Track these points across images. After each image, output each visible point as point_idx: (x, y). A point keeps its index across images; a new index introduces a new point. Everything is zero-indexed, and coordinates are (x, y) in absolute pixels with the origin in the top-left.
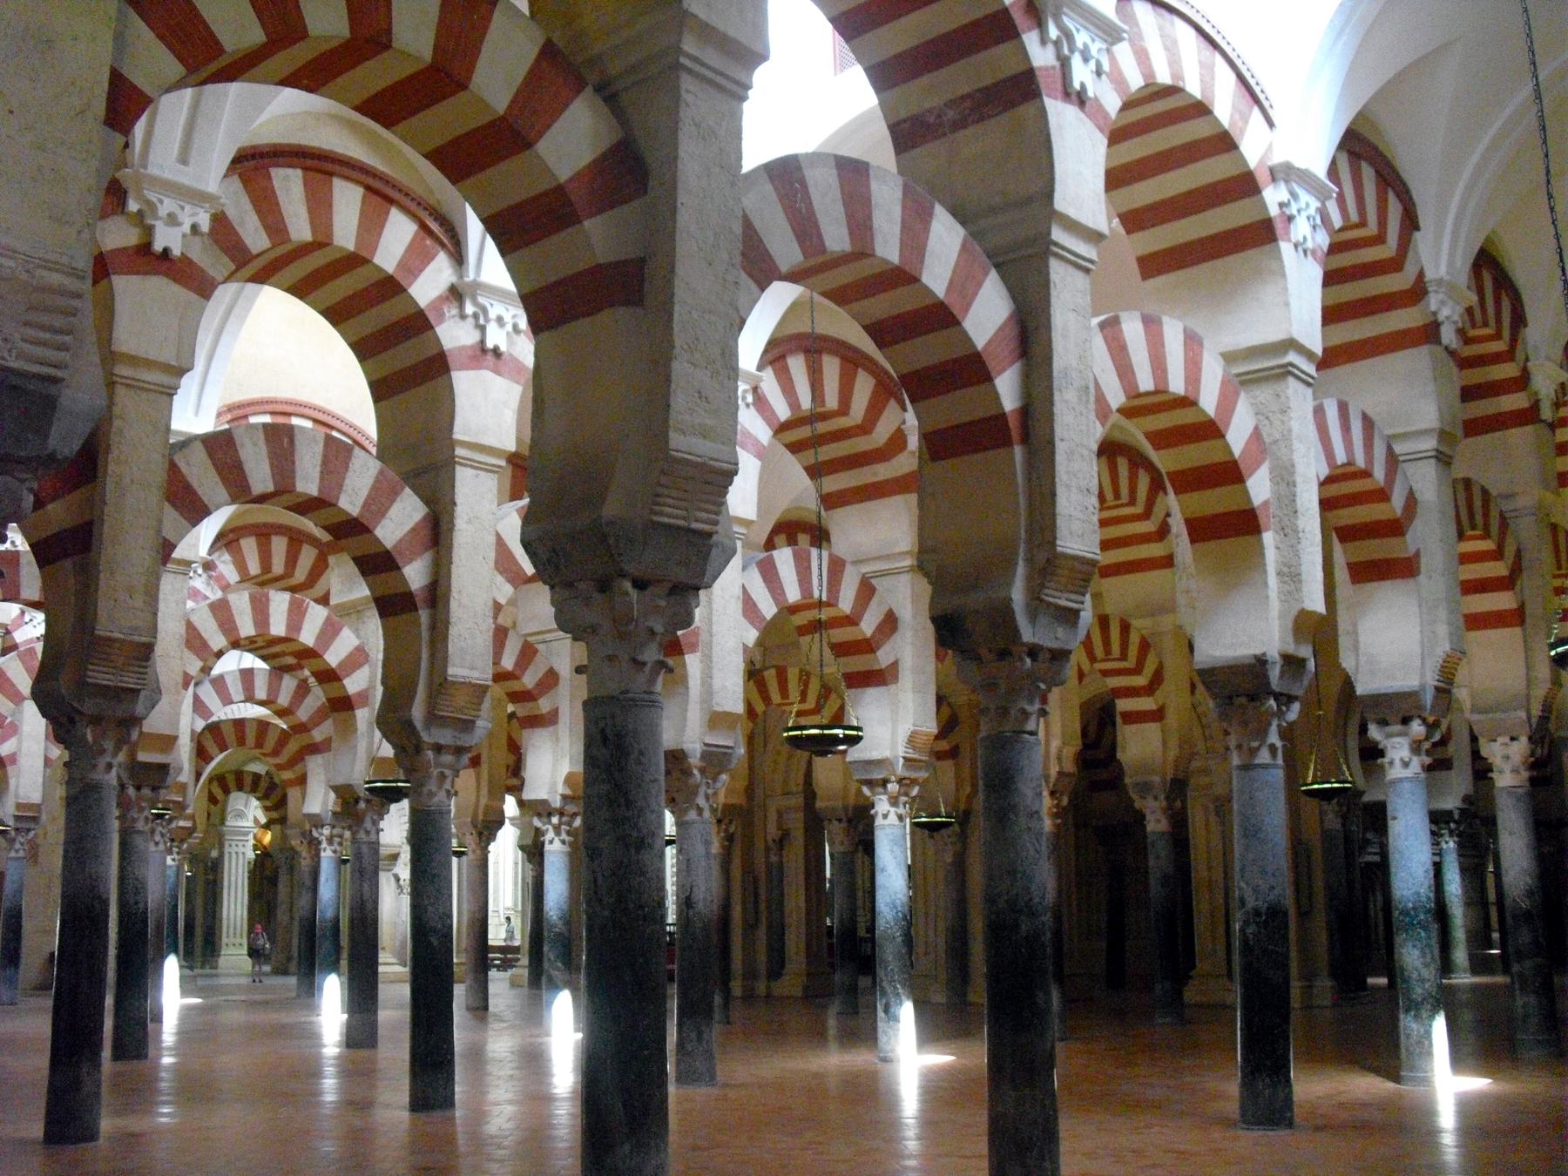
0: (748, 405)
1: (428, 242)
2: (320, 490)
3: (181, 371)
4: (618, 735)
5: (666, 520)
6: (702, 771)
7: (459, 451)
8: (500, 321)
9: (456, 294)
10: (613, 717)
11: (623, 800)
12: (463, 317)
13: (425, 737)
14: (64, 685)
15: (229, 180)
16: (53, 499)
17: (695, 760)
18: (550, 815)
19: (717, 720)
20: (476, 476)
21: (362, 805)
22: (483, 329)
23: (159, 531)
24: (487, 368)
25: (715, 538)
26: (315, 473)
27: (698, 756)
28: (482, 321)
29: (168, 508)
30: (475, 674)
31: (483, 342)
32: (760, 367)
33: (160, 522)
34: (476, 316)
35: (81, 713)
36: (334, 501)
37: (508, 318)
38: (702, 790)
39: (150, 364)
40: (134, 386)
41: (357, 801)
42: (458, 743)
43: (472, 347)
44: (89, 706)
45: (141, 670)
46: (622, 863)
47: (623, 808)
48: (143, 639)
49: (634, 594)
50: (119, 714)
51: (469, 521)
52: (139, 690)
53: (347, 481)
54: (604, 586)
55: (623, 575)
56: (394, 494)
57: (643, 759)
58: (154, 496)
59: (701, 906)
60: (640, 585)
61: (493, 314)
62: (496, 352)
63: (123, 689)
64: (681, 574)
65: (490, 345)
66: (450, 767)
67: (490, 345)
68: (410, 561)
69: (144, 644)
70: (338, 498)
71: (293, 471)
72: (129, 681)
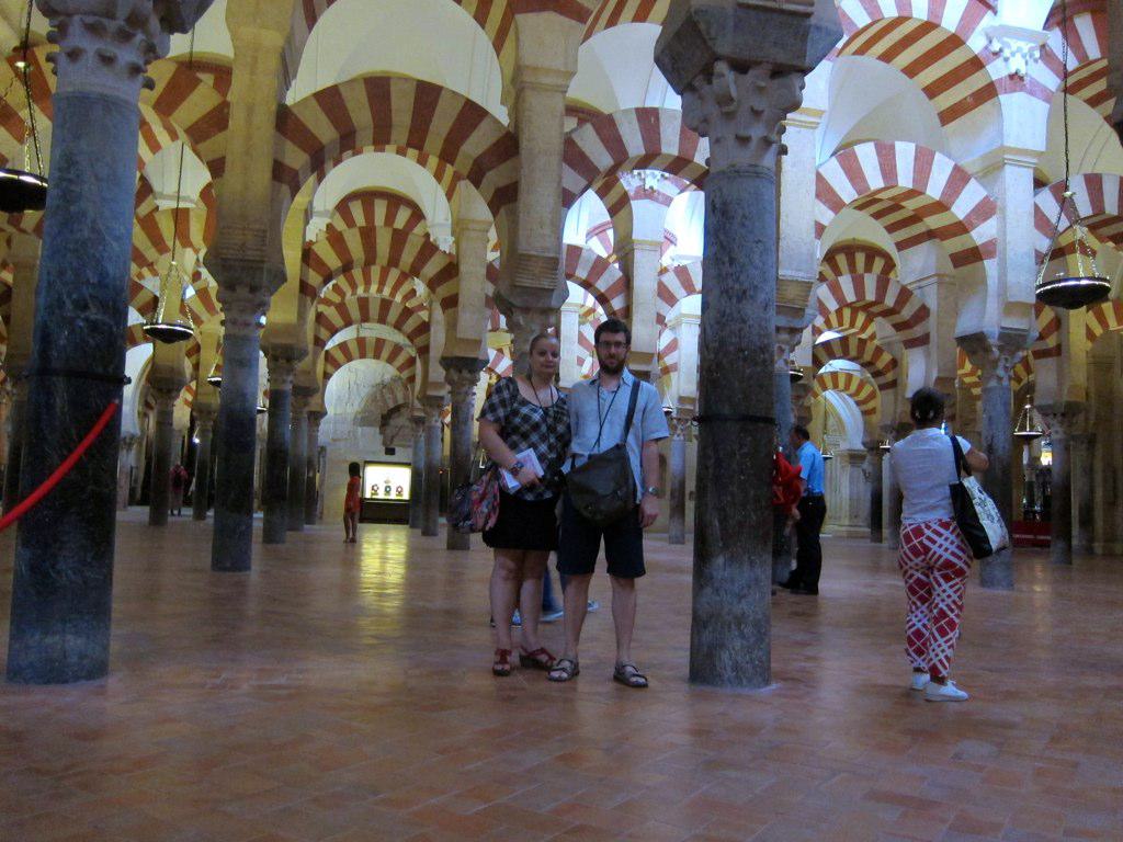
0: (1036, 61)
2: (680, 152)
3: (573, 74)
4: (725, 203)
6: (1001, 348)
10: (720, 190)
11: (727, 259)
16: (489, 169)
17: (993, 341)
19: (1010, 308)
20: (799, 132)
23: (560, 182)
25: (813, 21)
26: (676, 140)
27: (997, 336)
29: (566, 167)
30: (801, 274)
32: (1047, 25)
33: (561, 178)
38: (1001, 364)
39: (548, 71)
42: (792, 325)
44: (517, 302)
46: (725, 312)
47: (727, 265)
48: (551, 255)
49: (730, 76)
50: (540, 305)
51: (794, 165)
52: (553, 290)
54: (708, 73)
55: (718, 58)
57: (747, 223)
58: (555, 160)
59: (1000, 452)
60: (741, 67)
63: (541, 289)
64: (782, 57)
66: (787, 343)
69: (552, 258)
70: (694, 155)
71: (659, 140)
72: (546, 284)
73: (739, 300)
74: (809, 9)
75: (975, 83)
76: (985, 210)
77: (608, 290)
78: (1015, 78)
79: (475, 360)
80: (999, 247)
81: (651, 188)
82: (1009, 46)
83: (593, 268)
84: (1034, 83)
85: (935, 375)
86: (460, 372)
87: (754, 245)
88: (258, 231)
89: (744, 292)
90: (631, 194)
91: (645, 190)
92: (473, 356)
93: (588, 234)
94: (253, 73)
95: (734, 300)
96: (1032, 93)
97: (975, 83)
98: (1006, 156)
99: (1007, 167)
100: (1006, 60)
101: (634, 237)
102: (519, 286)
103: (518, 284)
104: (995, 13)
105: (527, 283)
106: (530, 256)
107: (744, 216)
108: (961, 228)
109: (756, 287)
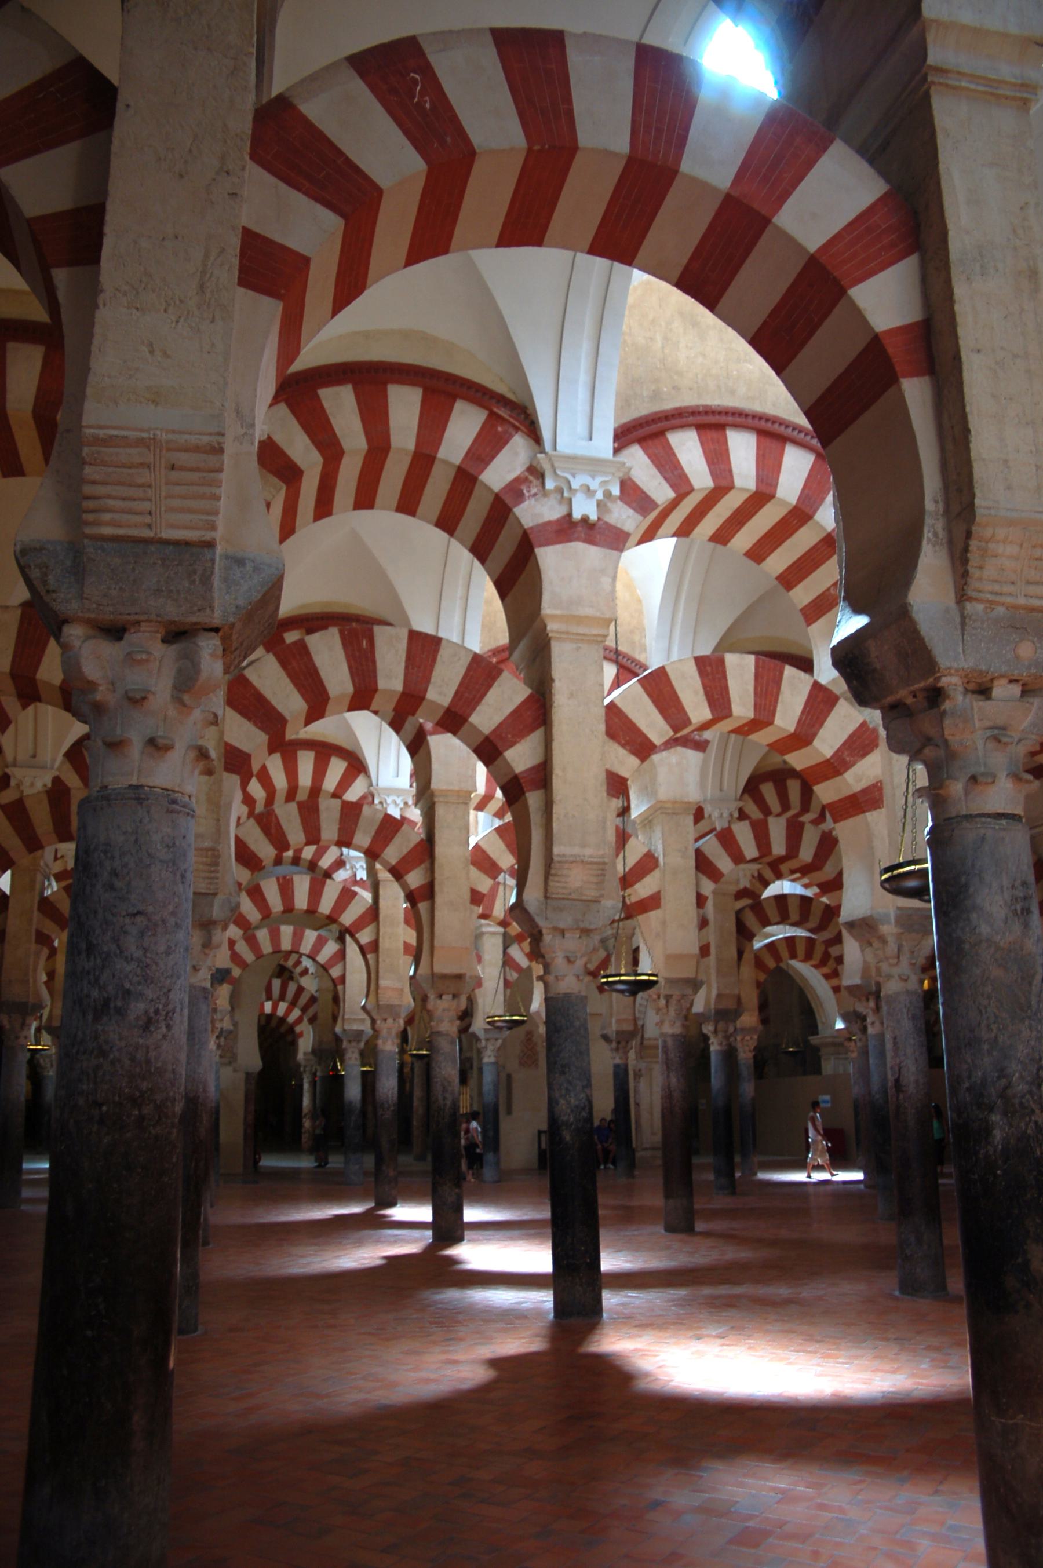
1: (500, 429)
5: (107, 531)
8: (588, 491)
9: (536, 473)
12: (545, 493)
15: (275, 408)
22: (570, 502)
24: (578, 539)
28: (566, 494)
31: (569, 515)
34: (560, 491)
37: (594, 484)
43: (558, 522)
45: (213, 875)
61: (575, 485)
65: (577, 515)
67: (577, 515)
68: (512, 744)
71: (375, 671)
73: (97, 1019)
74: (208, 536)
87: (128, 920)
89: (106, 1002)
95: (90, 1017)
107: (114, 873)
109: (128, 992)
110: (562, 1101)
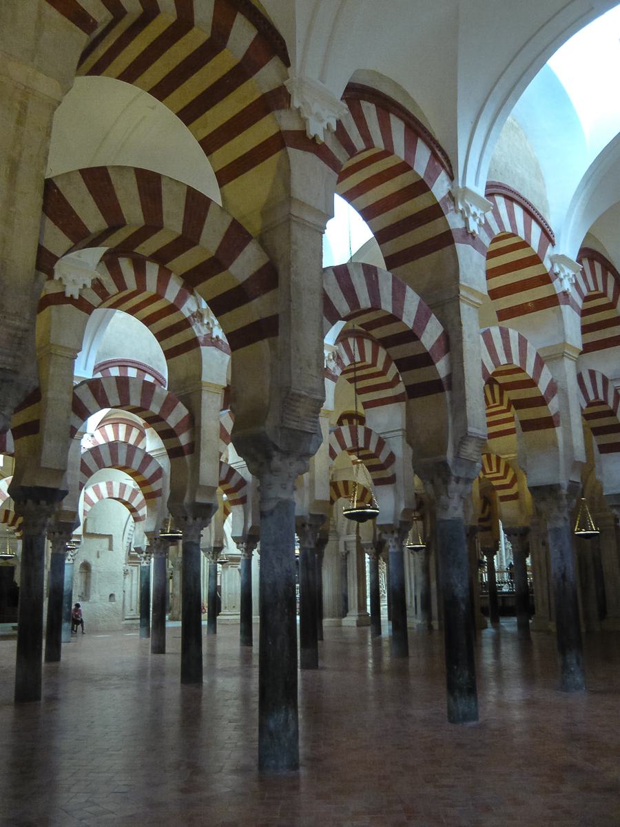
6: (567, 498)
7: (462, 292)
13: (454, 473)
14: (269, 427)
18: (393, 532)
19: (575, 465)
21: (307, 528)
22: (466, 220)
35: (276, 448)
36: (400, 318)
40: (304, 225)
41: (303, 525)
53: (405, 307)
56: (427, 318)
58: (317, 302)
62: (473, 235)
70: (402, 316)
75: (541, 292)
76: (553, 389)
77: (178, 425)
78: (565, 293)
79: (55, 491)
80: (562, 417)
81: (217, 337)
82: (563, 271)
83: (166, 403)
84: (574, 301)
85: (402, 507)
86: (38, 503)
88: (18, 328)
90: (201, 340)
91: (212, 338)
92: (51, 485)
93: (94, 370)
94: (20, 122)
96: (572, 307)
97: (541, 292)
98: (566, 351)
99: (565, 358)
100: (561, 280)
101: (204, 379)
102: (287, 428)
103: (286, 426)
104: (553, 245)
105: (294, 425)
106: (300, 396)
108: (542, 401)
110: (460, 585)
